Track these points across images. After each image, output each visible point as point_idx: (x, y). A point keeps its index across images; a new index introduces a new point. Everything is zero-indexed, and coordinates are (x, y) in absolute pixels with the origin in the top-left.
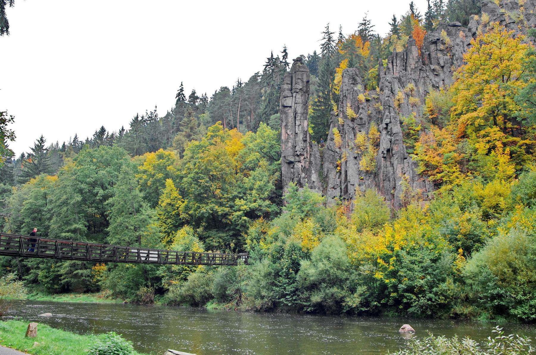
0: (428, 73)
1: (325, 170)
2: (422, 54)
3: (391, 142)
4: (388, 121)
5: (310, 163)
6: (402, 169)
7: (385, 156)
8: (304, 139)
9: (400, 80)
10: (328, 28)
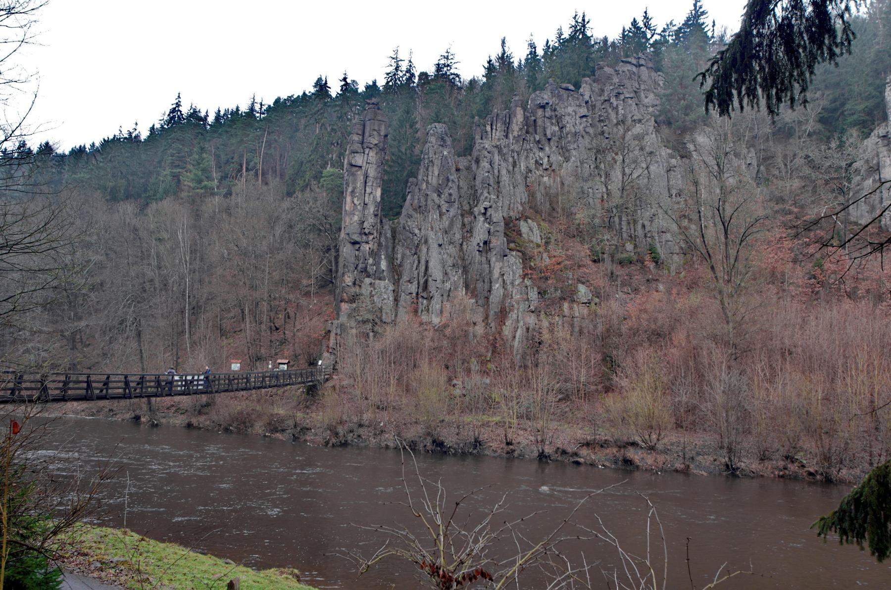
0: (532, 145)
1: (399, 256)
2: (526, 118)
3: (489, 232)
4: (487, 204)
5: (380, 245)
6: (501, 269)
7: (481, 249)
9: (500, 151)
10: (396, 52)
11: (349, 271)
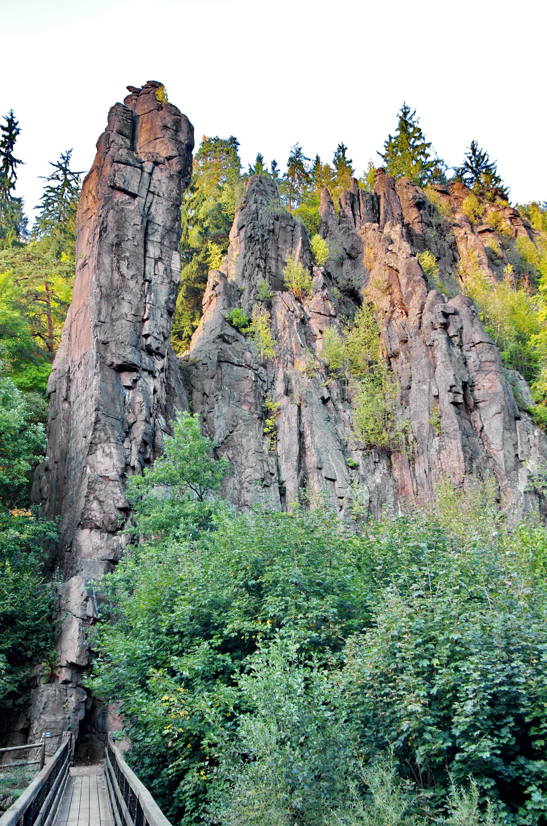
7: (460, 399)
8: (171, 306)
11: (108, 440)
